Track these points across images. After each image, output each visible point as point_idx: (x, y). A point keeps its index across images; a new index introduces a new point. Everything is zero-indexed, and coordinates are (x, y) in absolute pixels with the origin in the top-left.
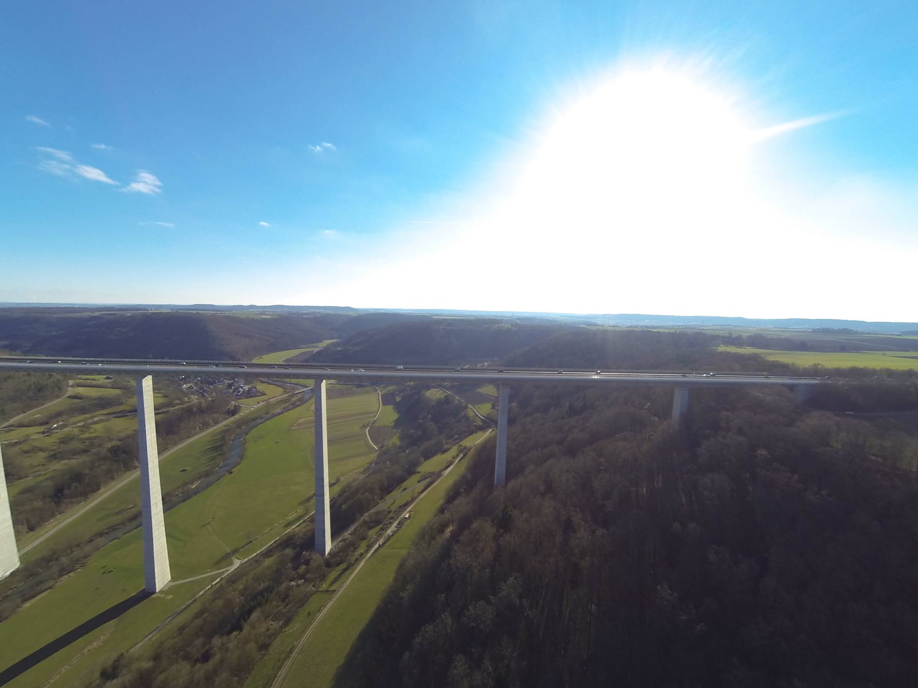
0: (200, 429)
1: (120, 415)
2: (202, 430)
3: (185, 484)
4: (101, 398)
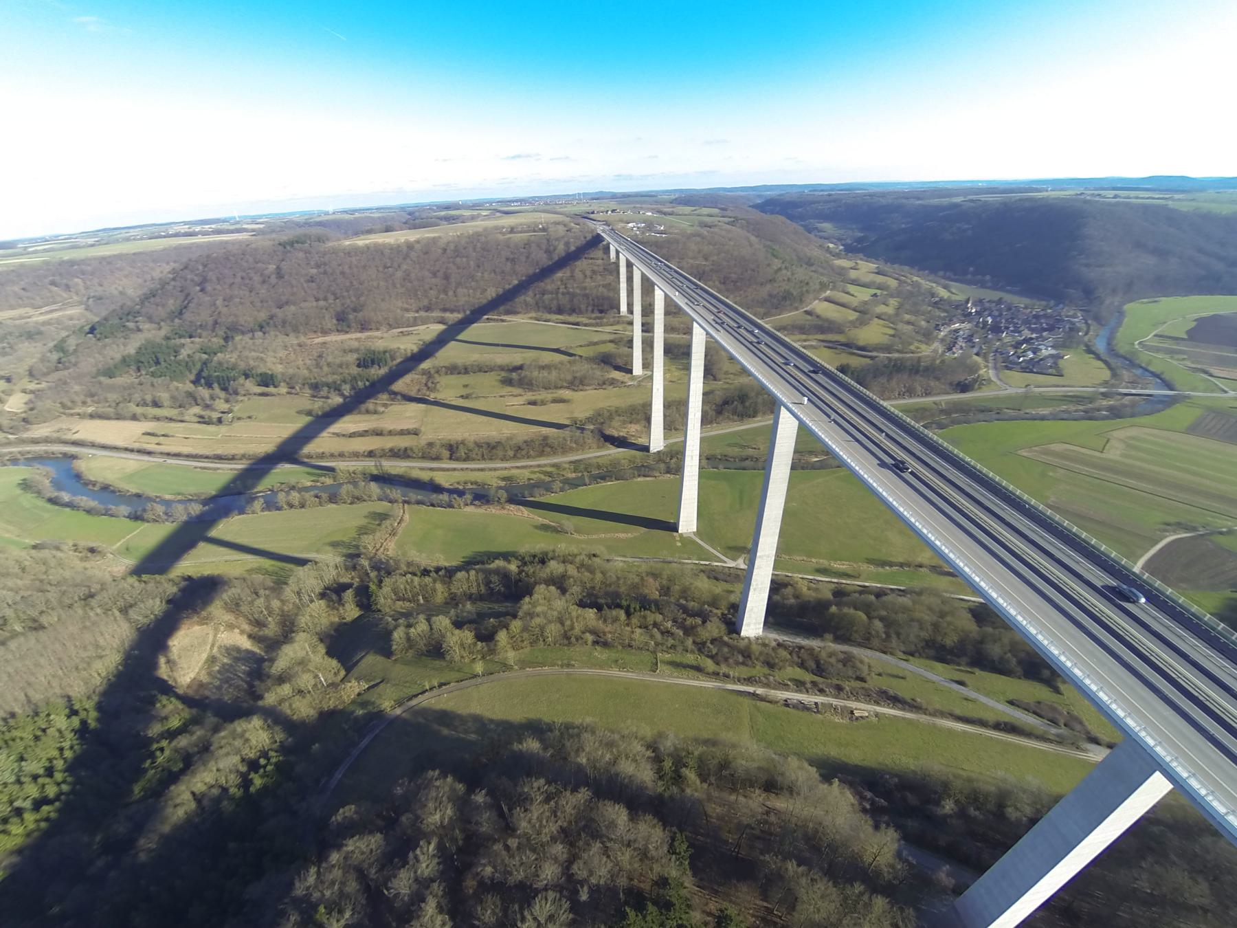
1: (831, 345)
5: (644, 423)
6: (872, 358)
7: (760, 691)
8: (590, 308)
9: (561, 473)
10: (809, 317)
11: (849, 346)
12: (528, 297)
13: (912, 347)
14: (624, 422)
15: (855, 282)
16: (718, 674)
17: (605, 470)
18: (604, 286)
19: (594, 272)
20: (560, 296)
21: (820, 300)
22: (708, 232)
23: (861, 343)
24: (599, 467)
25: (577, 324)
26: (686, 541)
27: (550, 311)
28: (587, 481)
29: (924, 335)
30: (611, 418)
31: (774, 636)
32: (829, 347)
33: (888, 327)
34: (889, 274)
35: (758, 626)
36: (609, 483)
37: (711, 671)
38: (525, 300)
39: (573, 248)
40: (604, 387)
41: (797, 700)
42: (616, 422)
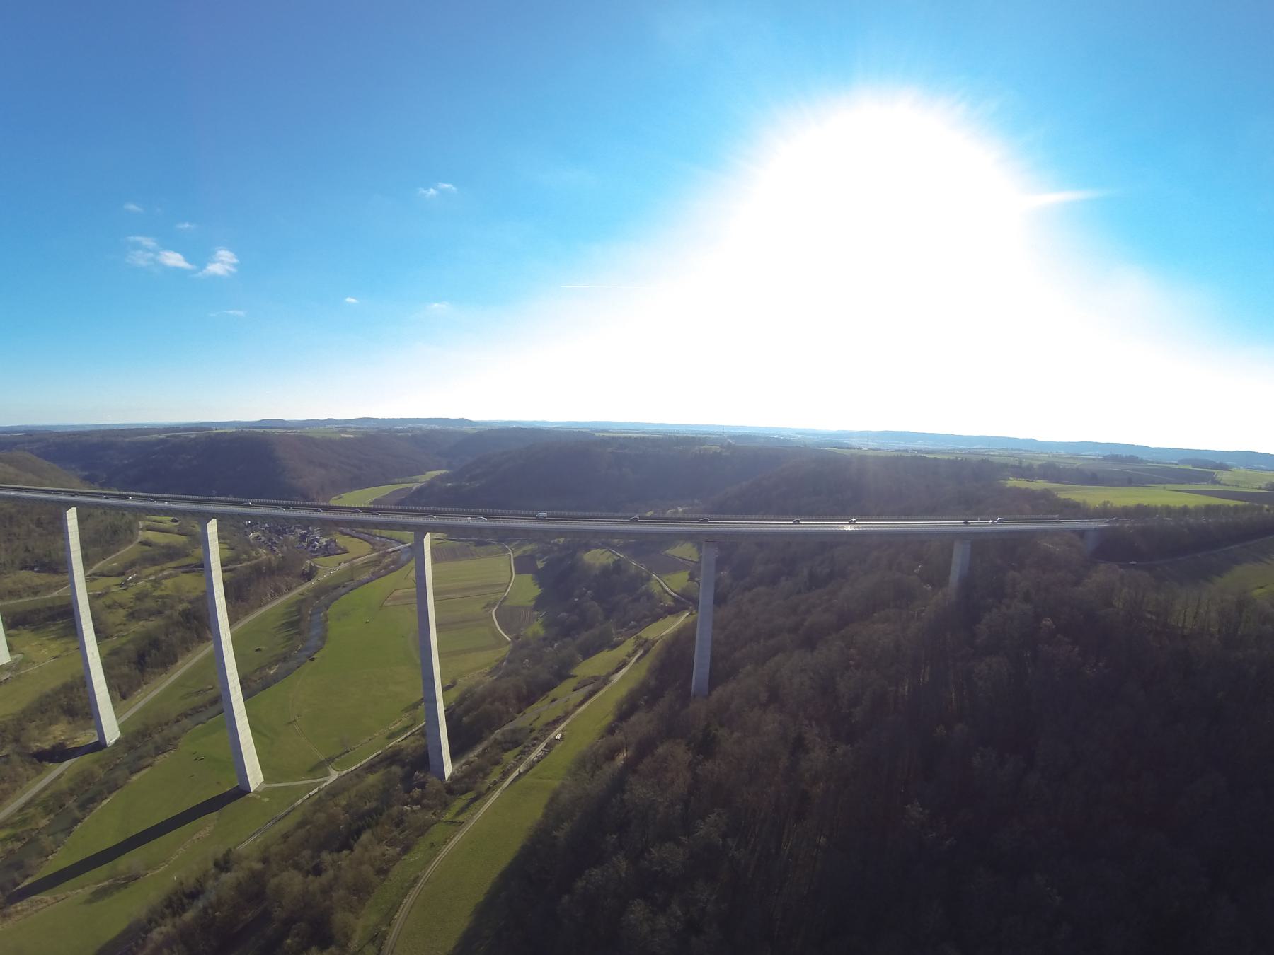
0: (272, 596)
1: (187, 570)
2: (274, 597)
3: (262, 668)
4: (168, 547)
32: (187, 572)
36: (105, 802)
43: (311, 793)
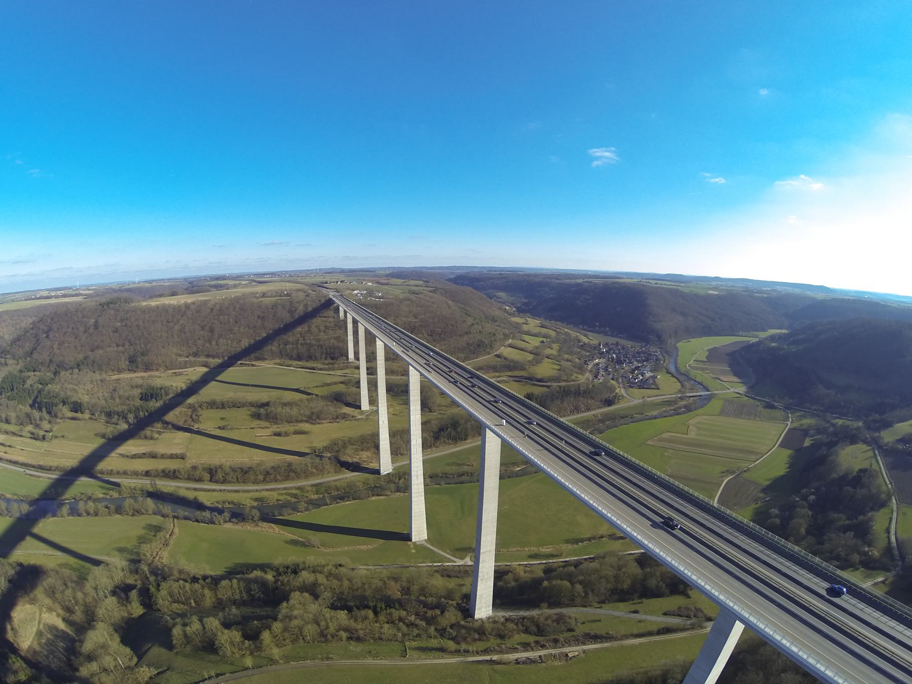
1: (517, 379)
5: (373, 450)
6: (548, 387)
7: (495, 657)
8: (324, 356)
9: (305, 495)
10: (499, 359)
11: (531, 379)
12: (274, 347)
13: (573, 377)
14: (357, 450)
15: (528, 333)
16: (459, 651)
17: (343, 491)
18: (336, 338)
19: (326, 327)
20: (299, 346)
21: (505, 346)
22: (416, 297)
23: (539, 377)
24: (337, 489)
25: (313, 369)
26: (419, 547)
27: (291, 358)
28: (328, 501)
29: (579, 368)
30: (345, 446)
31: (502, 614)
33: (555, 364)
34: (549, 327)
35: (489, 609)
36: (347, 503)
37: (453, 649)
38: (271, 350)
39: (310, 309)
40: (337, 420)
41: (525, 657)
42: (350, 450)
43: (435, 564)
